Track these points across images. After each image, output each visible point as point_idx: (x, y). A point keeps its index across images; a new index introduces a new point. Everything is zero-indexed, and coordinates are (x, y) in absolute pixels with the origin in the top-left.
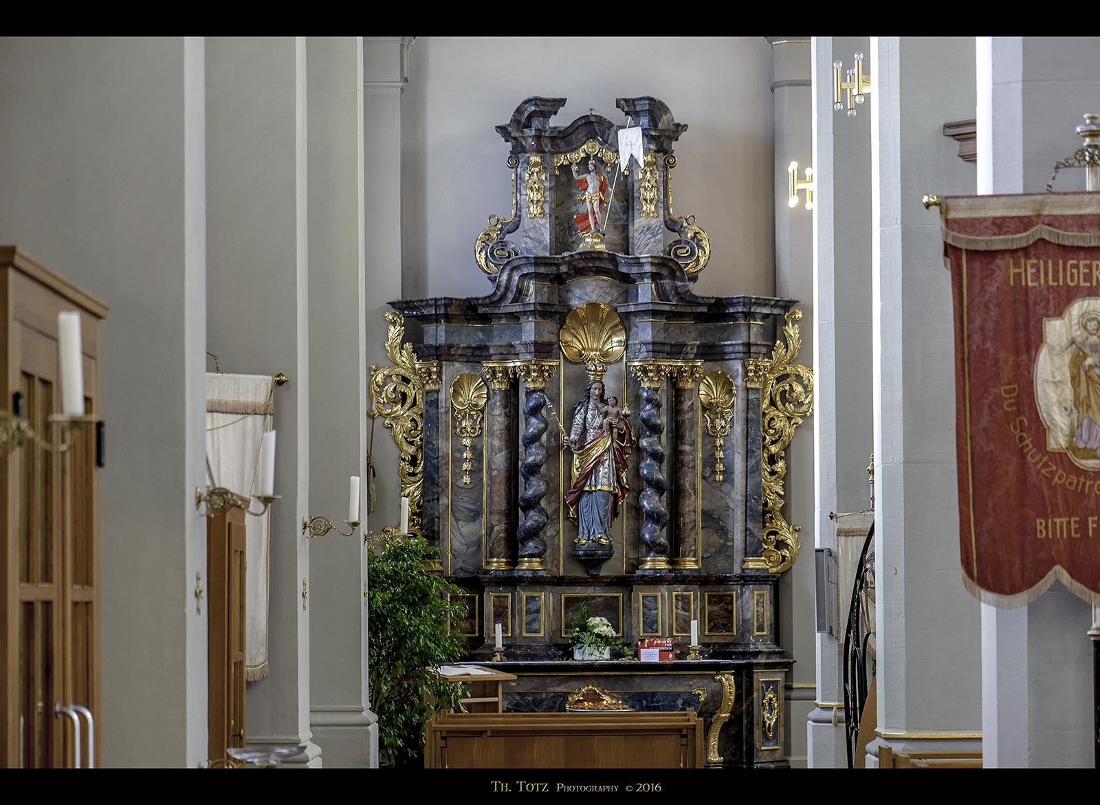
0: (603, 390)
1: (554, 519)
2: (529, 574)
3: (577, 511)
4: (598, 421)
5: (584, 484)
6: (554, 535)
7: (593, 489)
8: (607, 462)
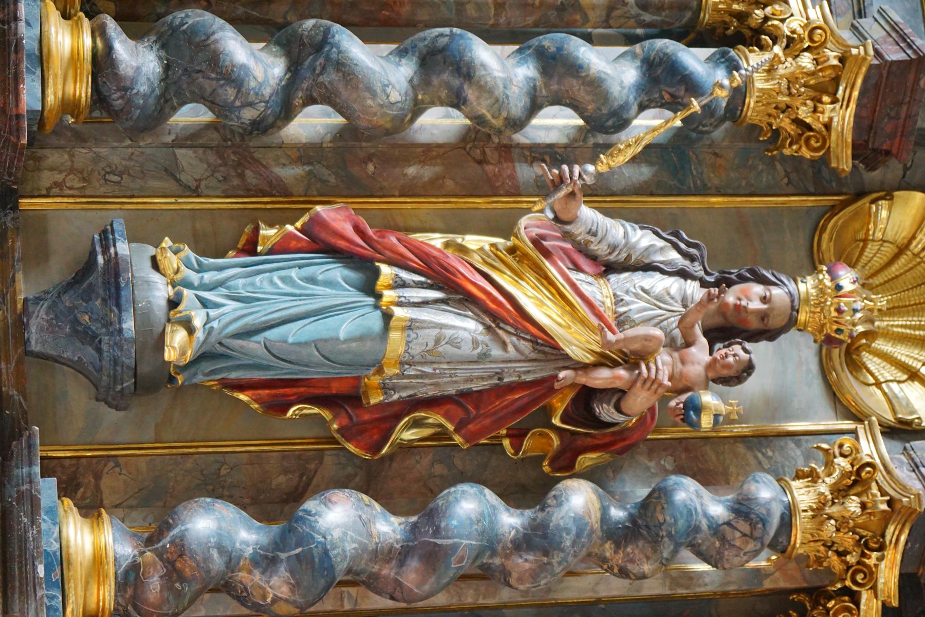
1: (241, 176)
3: (281, 248)
4: (636, 307)
5: (397, 262)
6: (183, 177)
7: (389, 295)
8: (496, 352)
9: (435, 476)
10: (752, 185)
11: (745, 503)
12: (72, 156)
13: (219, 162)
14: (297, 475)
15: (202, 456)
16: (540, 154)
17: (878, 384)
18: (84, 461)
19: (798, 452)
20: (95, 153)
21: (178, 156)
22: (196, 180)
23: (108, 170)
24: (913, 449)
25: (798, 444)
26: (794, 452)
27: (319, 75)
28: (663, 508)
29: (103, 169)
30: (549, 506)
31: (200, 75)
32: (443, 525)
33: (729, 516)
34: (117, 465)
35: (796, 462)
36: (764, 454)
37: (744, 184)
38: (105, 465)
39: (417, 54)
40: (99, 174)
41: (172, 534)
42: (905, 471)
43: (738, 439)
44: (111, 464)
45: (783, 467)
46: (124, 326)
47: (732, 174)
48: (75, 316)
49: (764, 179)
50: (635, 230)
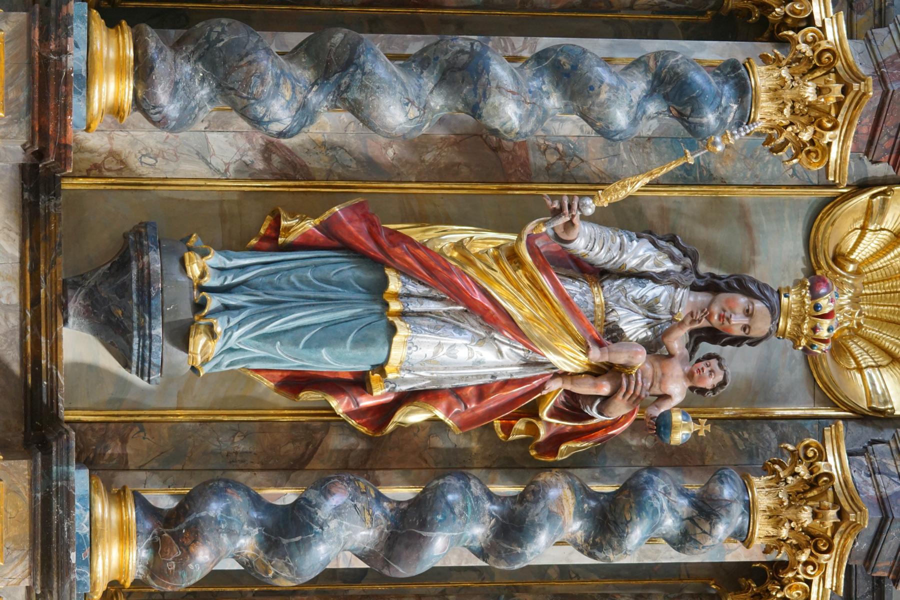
0: (737, 341)
2: (75, 60)
5: (406, 272)
6: (214, 161)
7: (395, 306)
9: (430, 448)
10: (756, 176)
11: (708, 502)
12: (111, 139)
13: (248, 146)
14: (304, 443)
15: (218, 423)
16: (553, 142)
17: (860, 369)
18: (112, 426)
19: (773, 435)
20: (132, 136)
21: (210, 140)
22: (226, 164)
23: (144, 152)
24: (874, 453)
25: (774, 429)
26: (769, 434)
27: (343, 92)
28: (631, 507)
29: (139, 152)
30: (528, 501)
31: (233, 92)
32: (429, 518)
33: (692, 512)
34: (142, 430)
35: (770, 444)
36: (740, 436)
37: (749, 175)
38: (131, 430)
39: (438, 67)
40: (136, 156)
41: (187, 520)
42: (863, 475)
43: (717, 422)
44: (137, 429)
45: (757, 449)
46: (153, 332)
47: (739, 165)
48: (109, 307)
49: (770, 170)
50: (632, 241)
